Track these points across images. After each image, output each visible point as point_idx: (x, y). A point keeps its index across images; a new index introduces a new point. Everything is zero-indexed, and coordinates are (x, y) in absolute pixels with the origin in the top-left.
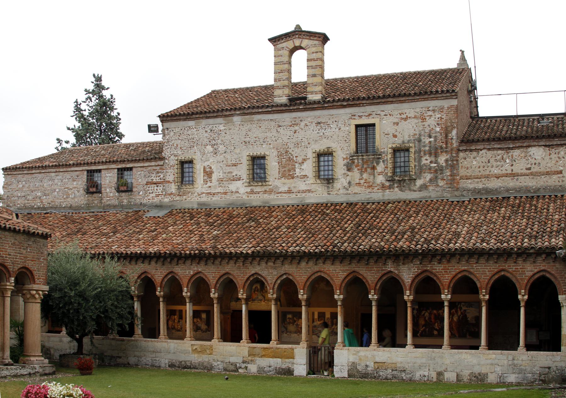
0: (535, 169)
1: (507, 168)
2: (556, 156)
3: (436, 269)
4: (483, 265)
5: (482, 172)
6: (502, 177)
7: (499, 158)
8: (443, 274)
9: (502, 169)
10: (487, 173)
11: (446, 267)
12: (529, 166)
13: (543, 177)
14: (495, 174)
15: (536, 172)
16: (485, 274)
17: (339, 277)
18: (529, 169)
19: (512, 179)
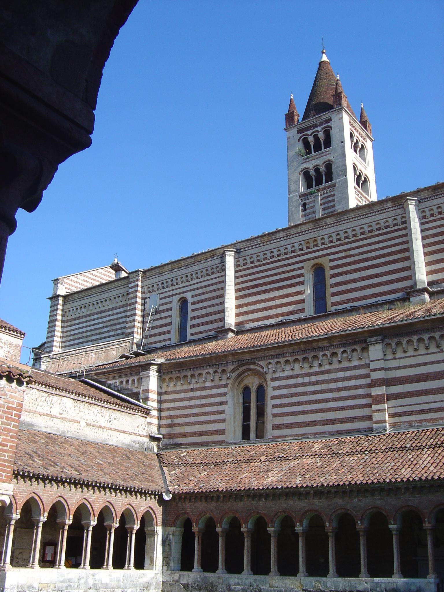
0: (65, 415)
1: (46, 410)
2: (78, 408)
3: (91, 498)
4: (119, 499)
5: (31, 407)
6: (44, 415)
7: (43, 399)
8: (95, 503)
9: (44, 408)
10: (35, 409)
11: (97, 497)
12: (61, 412)
13: (69, 422)
14: (39, 412)
15: (65, 418)
16: (120, 506)
17: (21, 497)
18: (61, 414)
19: (50, 419)
